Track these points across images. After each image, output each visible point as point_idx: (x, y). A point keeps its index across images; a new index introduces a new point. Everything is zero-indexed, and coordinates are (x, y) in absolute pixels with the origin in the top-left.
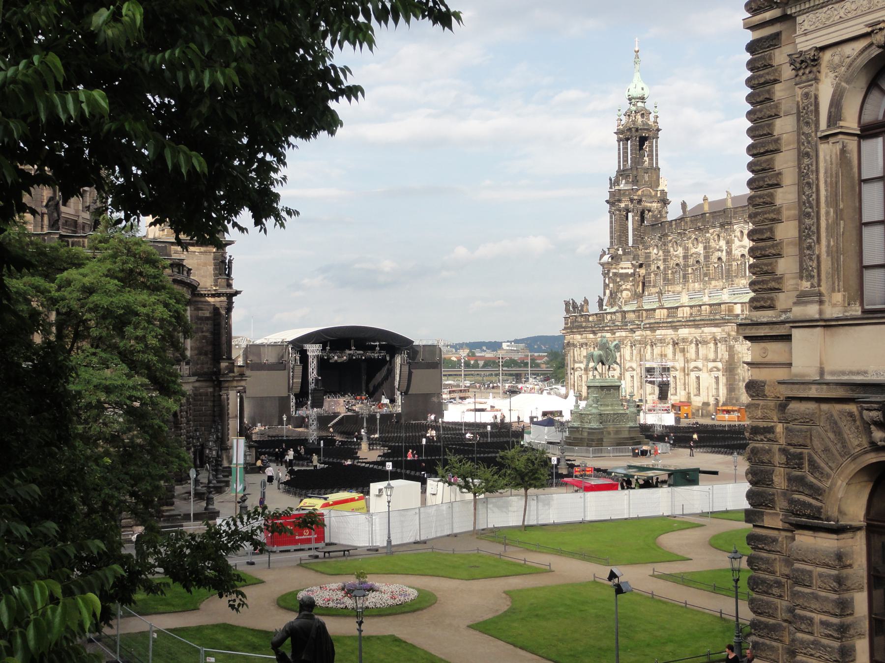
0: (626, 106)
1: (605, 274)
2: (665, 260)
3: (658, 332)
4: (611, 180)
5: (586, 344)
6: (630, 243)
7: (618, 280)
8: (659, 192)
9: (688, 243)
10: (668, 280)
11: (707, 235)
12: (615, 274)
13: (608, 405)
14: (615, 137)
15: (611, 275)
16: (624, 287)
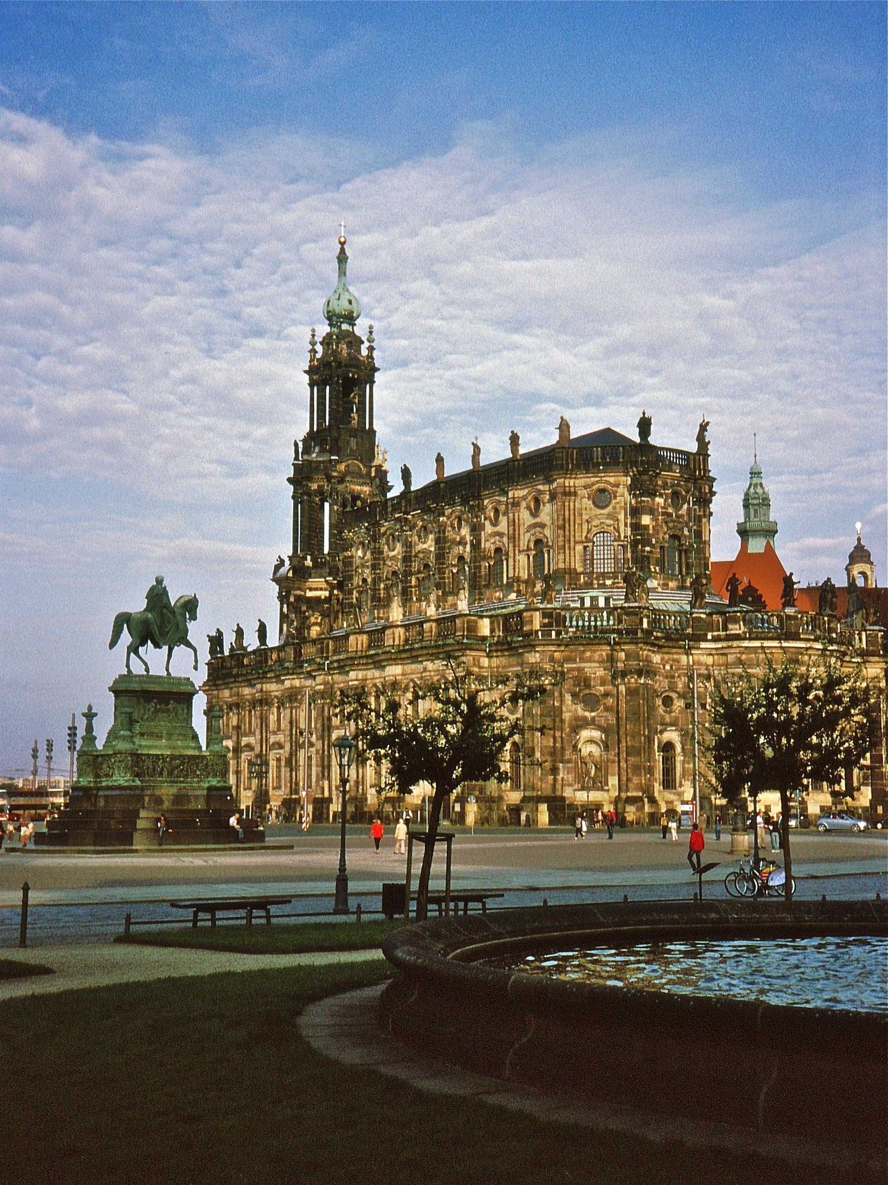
0: (324, 329)
1: (282, 598)
2: (374, 567)
3: (352, 675)
4: (296, 445)
5: (237, 706)
6: (326, 550)
7: (304, 608)
8: (373, 469)
9: (411, 536)
10: (379, 600)
11: (441, 519)
12: (298, 598)
13: (159, 737)
14: (306, 378)
15: (292, 599)
16: (313, 620)
